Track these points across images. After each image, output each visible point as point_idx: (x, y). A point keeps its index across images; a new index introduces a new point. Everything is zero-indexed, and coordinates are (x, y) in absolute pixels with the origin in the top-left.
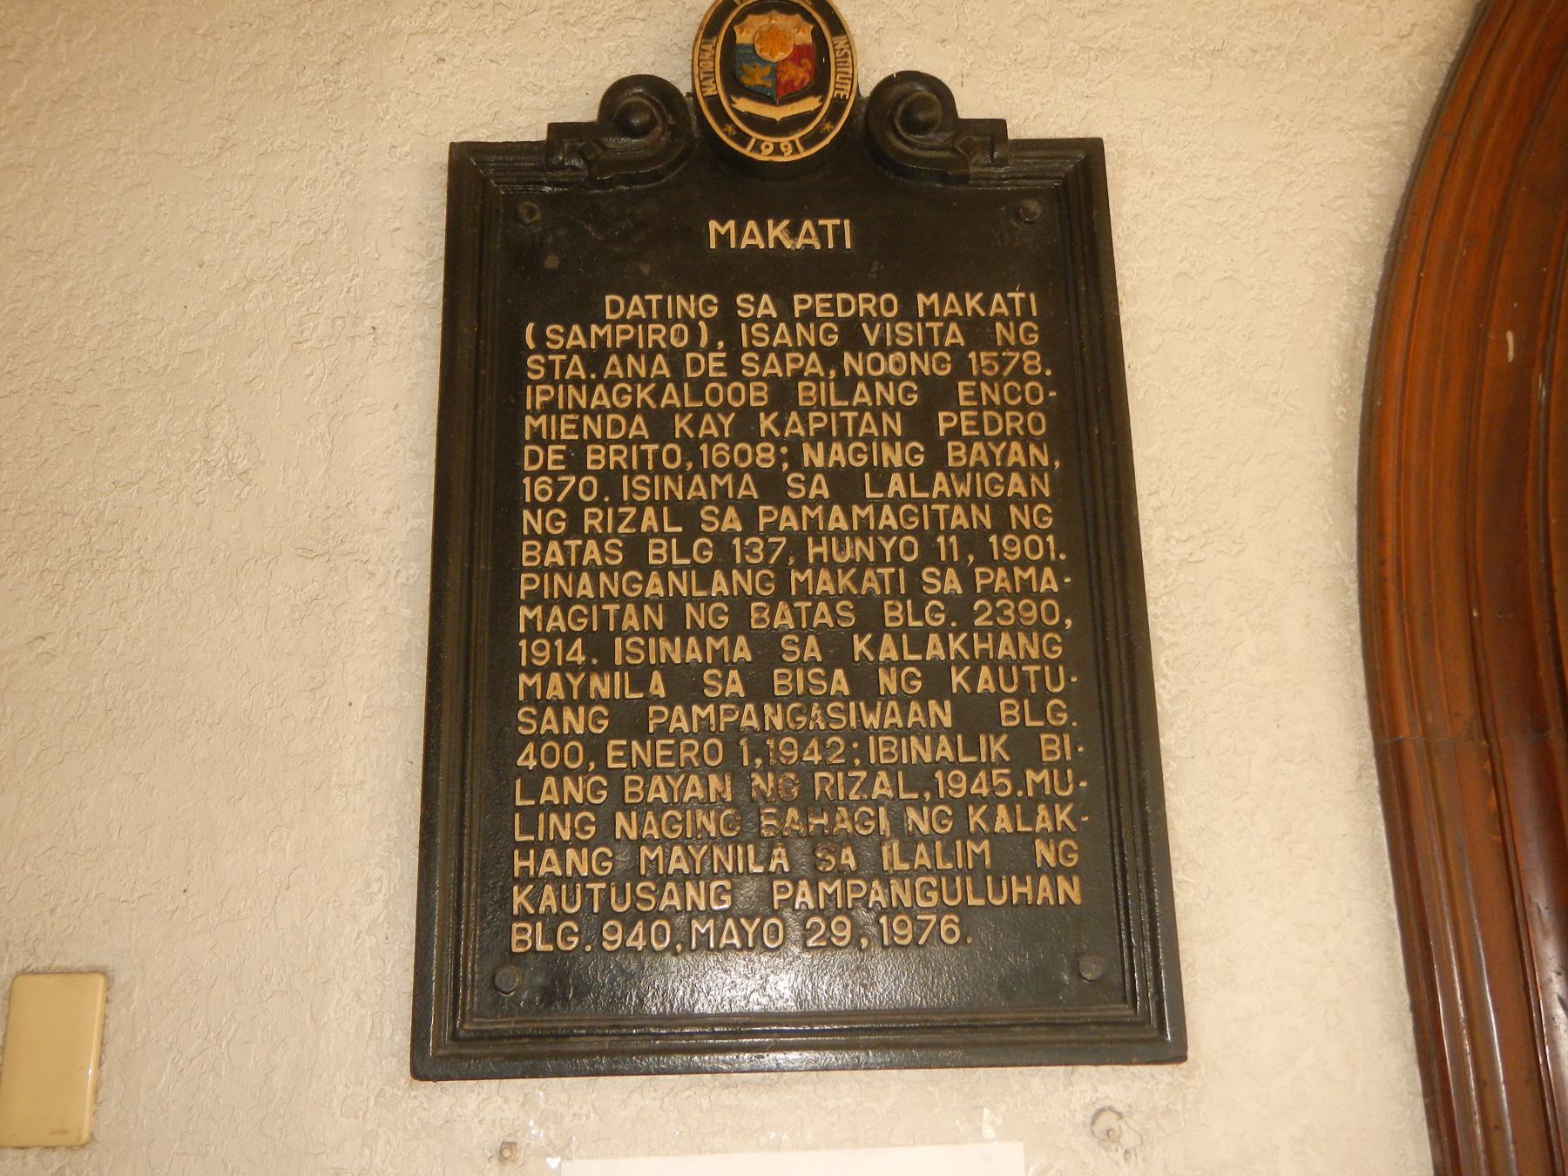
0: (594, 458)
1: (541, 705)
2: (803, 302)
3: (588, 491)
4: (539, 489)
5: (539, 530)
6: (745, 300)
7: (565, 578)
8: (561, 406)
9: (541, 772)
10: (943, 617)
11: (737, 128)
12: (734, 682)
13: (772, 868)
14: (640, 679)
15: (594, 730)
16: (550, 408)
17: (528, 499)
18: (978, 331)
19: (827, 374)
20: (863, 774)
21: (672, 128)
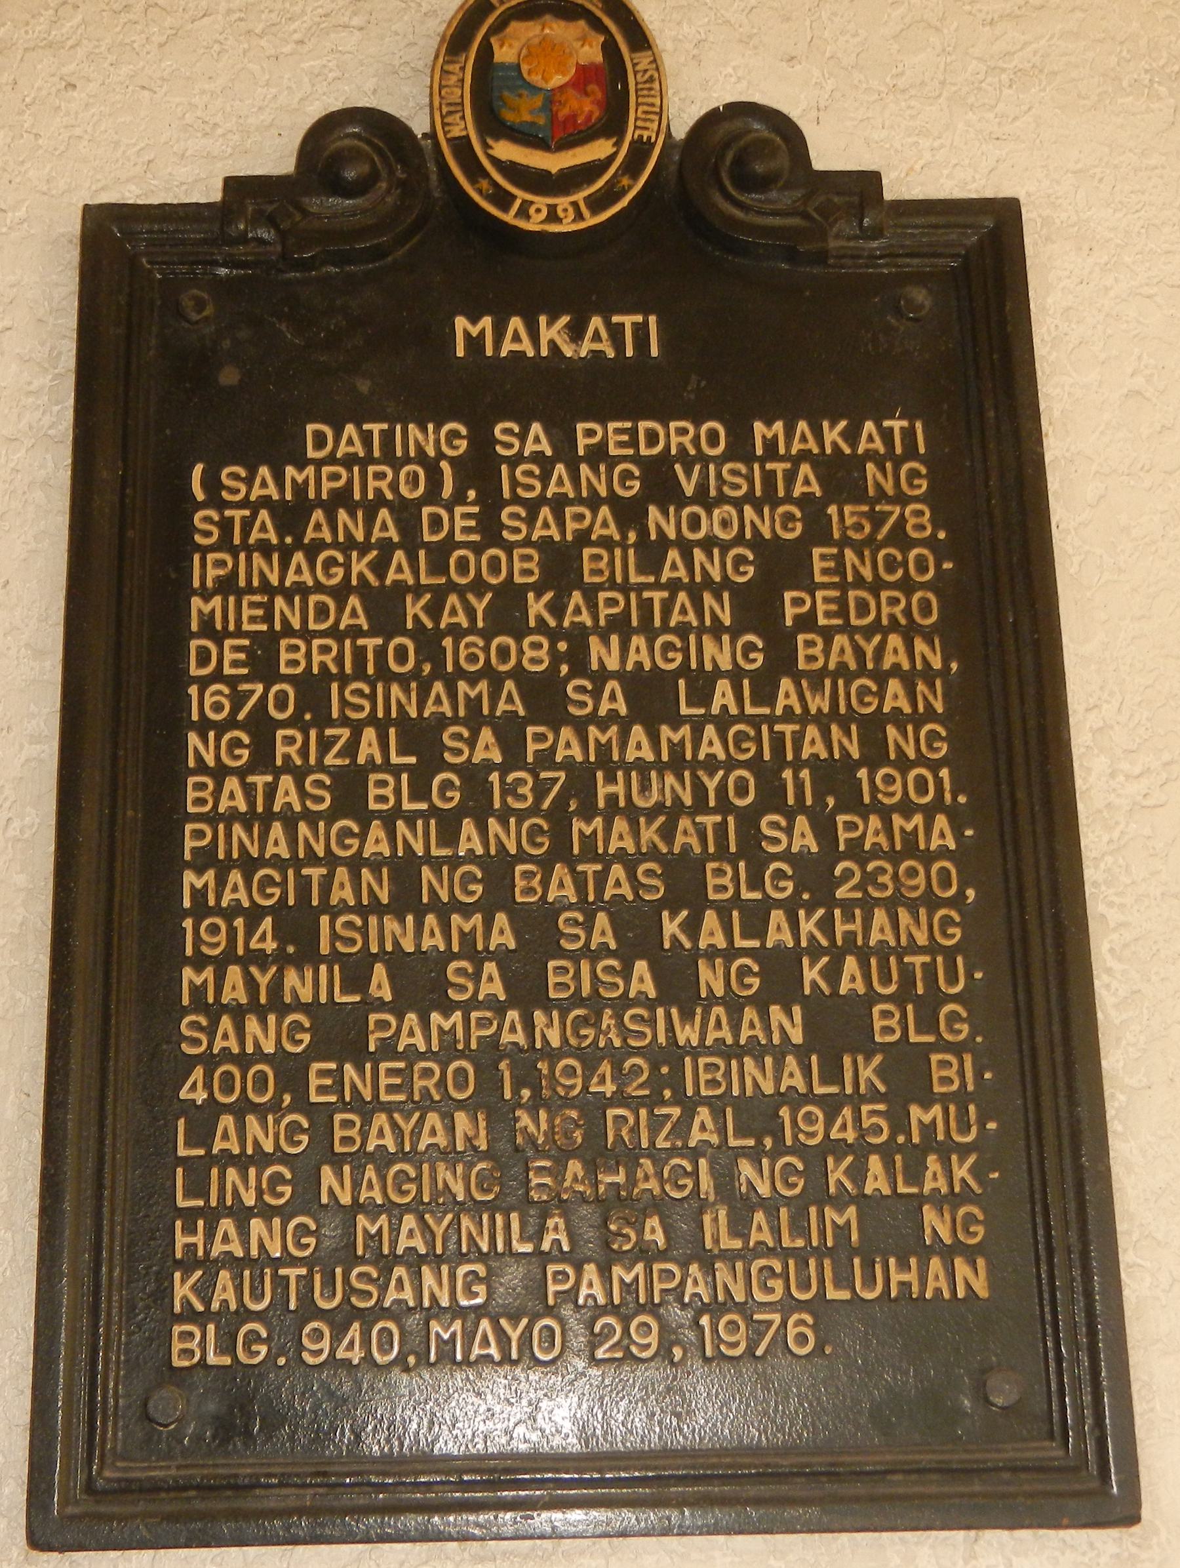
1: (215, 1012)
2: (590, 433)
3: (281, 704)
4: (210, 702)
5: (210, 760)
7: (249, 829)
8: (242, 583)
9: (213, 1109)
10: (790, 886)
11: (495, 184)
12: (490, 979)
13: (546, 1246)
14: (356, 974)
16: (227, 586)
17: (195, 717)
18: (842, 476)
19: (624, 537)
20: (676, 1112)
21: (402, 184)
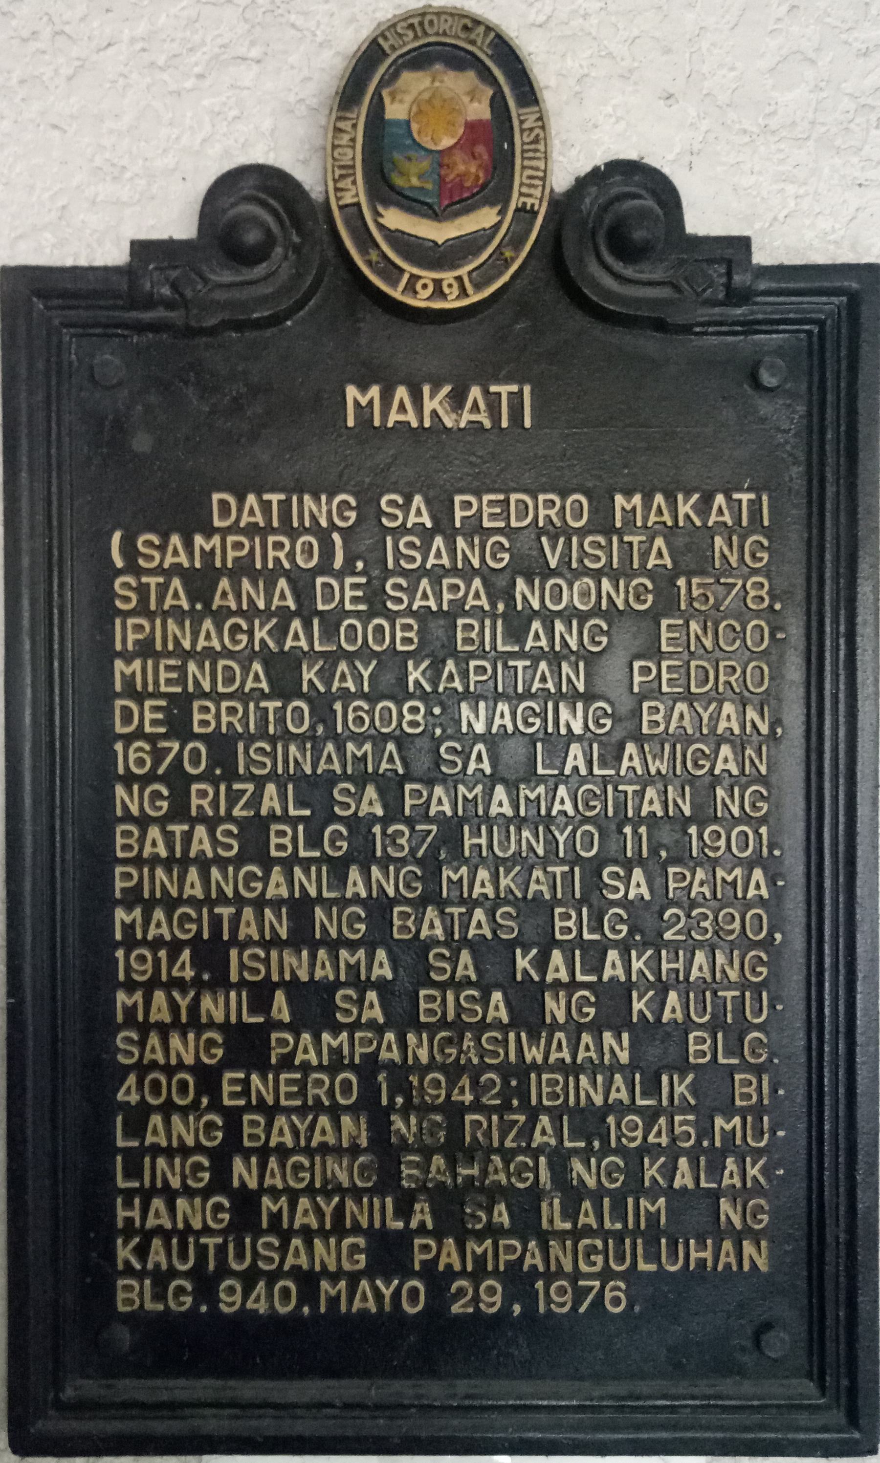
0: (201, 719)
1: (144, 1029)
2: (467, 505)
3: (196, 762)
4: (131, 757)
5: (135, 810)
6: (391, 503)
7: (169, 871)
8: (159, 647)
9: (143, 1111)
10: (625, 928)
11: (385, 256)
12: (372, 1006)
13: (414, 1224)
14: (260, 995)
15: (206, 1060)
16: (146, 649)
17: (121, 770)
18: (692, 551)
19: (494, 605)
20: (522, 1118)
21: (297, 249)
